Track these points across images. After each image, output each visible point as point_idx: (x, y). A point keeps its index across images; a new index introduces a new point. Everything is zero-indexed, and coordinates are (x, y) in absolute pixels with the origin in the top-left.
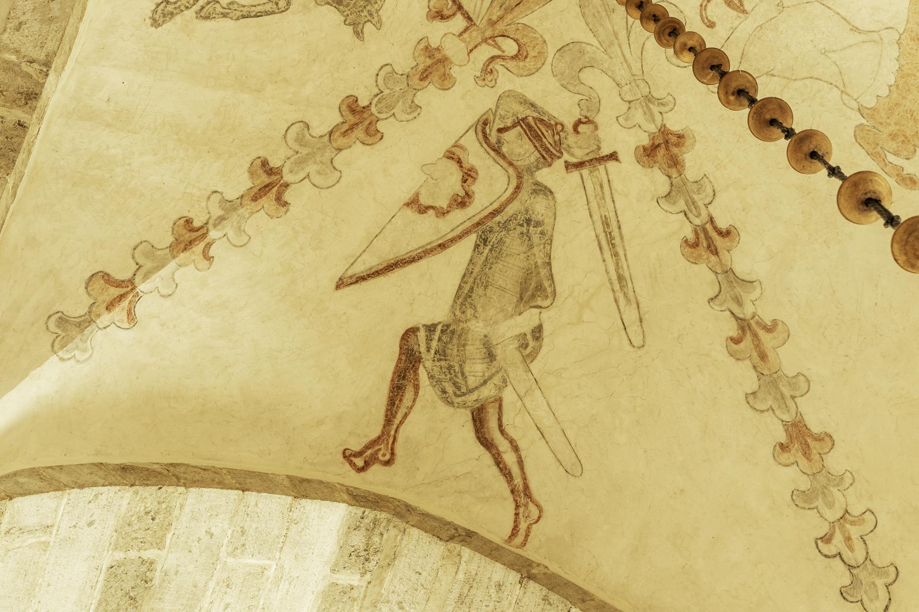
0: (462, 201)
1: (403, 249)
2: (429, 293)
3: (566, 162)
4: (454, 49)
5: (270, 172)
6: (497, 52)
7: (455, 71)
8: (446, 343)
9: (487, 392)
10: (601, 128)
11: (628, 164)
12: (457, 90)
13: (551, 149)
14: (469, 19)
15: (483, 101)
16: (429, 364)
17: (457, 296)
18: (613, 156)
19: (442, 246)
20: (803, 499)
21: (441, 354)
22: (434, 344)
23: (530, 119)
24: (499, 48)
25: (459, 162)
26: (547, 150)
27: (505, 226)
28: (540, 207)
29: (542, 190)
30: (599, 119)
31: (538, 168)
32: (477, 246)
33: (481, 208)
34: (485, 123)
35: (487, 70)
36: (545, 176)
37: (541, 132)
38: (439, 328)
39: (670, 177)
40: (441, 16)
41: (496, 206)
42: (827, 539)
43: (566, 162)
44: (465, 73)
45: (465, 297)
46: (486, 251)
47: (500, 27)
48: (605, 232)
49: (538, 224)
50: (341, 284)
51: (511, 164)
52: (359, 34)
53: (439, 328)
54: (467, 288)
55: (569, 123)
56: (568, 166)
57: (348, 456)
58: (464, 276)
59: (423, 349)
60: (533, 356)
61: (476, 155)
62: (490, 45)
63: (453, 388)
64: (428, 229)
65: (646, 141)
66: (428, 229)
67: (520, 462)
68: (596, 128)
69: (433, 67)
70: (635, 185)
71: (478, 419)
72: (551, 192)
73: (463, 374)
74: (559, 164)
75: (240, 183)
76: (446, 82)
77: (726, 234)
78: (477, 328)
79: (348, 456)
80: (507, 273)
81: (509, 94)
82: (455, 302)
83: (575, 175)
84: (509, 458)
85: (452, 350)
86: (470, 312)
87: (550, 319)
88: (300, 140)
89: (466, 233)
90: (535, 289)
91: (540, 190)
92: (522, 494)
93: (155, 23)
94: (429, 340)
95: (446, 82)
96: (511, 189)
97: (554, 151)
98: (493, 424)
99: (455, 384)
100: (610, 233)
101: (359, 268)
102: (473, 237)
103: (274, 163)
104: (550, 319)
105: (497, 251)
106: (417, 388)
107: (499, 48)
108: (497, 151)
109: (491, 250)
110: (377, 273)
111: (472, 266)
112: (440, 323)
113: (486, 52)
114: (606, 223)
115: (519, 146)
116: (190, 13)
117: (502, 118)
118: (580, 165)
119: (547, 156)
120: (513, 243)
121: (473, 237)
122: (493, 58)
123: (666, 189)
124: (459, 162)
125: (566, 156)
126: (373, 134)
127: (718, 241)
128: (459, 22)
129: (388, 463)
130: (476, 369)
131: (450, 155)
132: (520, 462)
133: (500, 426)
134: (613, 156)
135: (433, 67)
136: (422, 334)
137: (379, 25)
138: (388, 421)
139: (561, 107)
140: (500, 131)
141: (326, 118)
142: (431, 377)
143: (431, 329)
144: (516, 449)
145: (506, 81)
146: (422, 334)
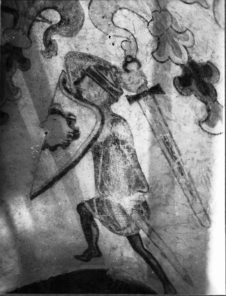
3: (127, 96)
6: (47, 25)
8: (101, 207)
10: (143, 65)
13: (114, 88)
16: (97, 216)
21: (101, 212)
22: (95, 208)
23: (92, 68)
24: (47, 21)
26: (111, 89)
27: (106, 143)
30: (140, 57)
31: (111, 104)
32: (95, 159)
33: (87, 136)
34: (64, 81)
38: (94, 200)
39: (206, 103)
41: (95, 133)
43: (127, 96)
46: (101, 160)
48: (167, 148)
49: (123, 142)
51: (93, 105)
53: (94, 200)
54: (99, 180)
55: (118, 63)
56: (131, 100)
58: (95, 175)
59: (91, 210)
62: (39, 21)
68: (140, 65)
72: (125, 120)
73: (116, 221)
74: (123, 100)
82: (97, 188)
83: (135, 104)
86: (106, 192)
91: (117, 119)
96: (99, 123)
97: (116, 89)
99: (114, 225)
100: (171, 149)
107: (47, 21)
109: (103, 159)
111: (97, 169)
112: (93, 198)
115: (93, 92)
117: (73, 74)
119: (114, 96)
121: (90, 156)
122: (46, 34)
123: (202, 115)
125: (126, 92)
140: (76, 83)
142: (101, 221)
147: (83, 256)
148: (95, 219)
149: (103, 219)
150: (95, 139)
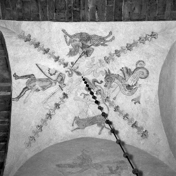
0: (51, 75)
1: (44, 71)
2: (39, 75)
4: (68, 66)
5: (48, 51)
7: (66, 67)
9: (29, 88)
11: (63, 92)
12: (64, 69)
14: (73, 66)
15: (64, 73)
17: (40, 79)
18: (62, 90)
19: (45, 75)
20: (34, 132)
21: (32, 80)
25: (56, 72)
27: (50, 81)
28: (54, 84)
29: (56, 83)
34: (61, 74)
35: (67, 71)
36: (57, 83)
37: (62, 80)
40: (72, 63)
42: (31, 137)
44: (66, 69)
45: (40, 80)
47: (72, 71)
50: (36, 64)
52: (67, 55)
55: (64, 83)
56: (59, 85)
57: (15, 74)
60: (36, 91)
61: (57, 74)
63: (28, 83)
64: (47, 72)
65: (65, 93)
66: (47, 72)
67: (22, 96)
69: (66, 65)
70: (60, 94)
71: (26, 88)
75: (45, 48)
76: (64, 67)
77: (59, 107)
78: (37, 83)
79: (15, 74)
80: (45, 84)
81: (65, 75)
83: (59, 87)
84: (22, 94)
85: (33, 81)
87: (41, 91)
88: (53, 53)
89: (48, 77)
90: (44, 88)
92: (19, 97)
93: (62, 30)
94: (33, 78)
95: (64, 67)
98: (26, 90)
101: (39, 66)
102: (47, 78)
103: (49, 51)
104: (41, 91)
105: (47, 81)
106: (27, 78)
108: (58, 76)
110: (39, 68)
113: (69, 70)
114: (55, 93)
115: (59, 80)
116: (65, 34)
118: (60, 87)
119: (59, 83)
120: (48, 83)
121: (47, 78)
122: (68, 71)
123: (61, 98)
124: (56, 72)
126: (56, 61)
127: (58, 107)
128: (72, 66)
129: (15, 79)
130: (32, 85)
131: (56, 71)
132: (22, 96)
133: (25, 92)
134: (62, 90)
135: (66, 65)
136: (34, 77)
137: (69, 57)
138: (21, 77)
139: (66, 82)
141: (56, 55)
142: (29, 80)
143: (35, 77)
144: (24, 94)
145: (67, 74)
146: (34, 77)
147: (16, 75)
148: (28, 79)
149: (30, 80)
150: (51, 79)
